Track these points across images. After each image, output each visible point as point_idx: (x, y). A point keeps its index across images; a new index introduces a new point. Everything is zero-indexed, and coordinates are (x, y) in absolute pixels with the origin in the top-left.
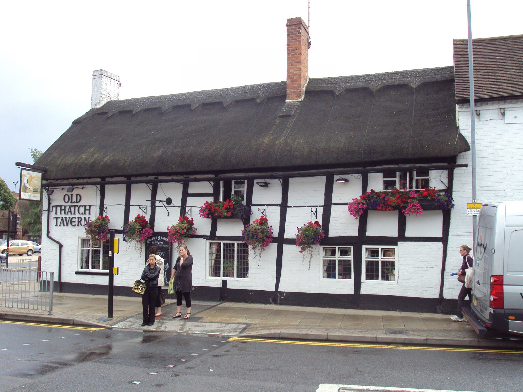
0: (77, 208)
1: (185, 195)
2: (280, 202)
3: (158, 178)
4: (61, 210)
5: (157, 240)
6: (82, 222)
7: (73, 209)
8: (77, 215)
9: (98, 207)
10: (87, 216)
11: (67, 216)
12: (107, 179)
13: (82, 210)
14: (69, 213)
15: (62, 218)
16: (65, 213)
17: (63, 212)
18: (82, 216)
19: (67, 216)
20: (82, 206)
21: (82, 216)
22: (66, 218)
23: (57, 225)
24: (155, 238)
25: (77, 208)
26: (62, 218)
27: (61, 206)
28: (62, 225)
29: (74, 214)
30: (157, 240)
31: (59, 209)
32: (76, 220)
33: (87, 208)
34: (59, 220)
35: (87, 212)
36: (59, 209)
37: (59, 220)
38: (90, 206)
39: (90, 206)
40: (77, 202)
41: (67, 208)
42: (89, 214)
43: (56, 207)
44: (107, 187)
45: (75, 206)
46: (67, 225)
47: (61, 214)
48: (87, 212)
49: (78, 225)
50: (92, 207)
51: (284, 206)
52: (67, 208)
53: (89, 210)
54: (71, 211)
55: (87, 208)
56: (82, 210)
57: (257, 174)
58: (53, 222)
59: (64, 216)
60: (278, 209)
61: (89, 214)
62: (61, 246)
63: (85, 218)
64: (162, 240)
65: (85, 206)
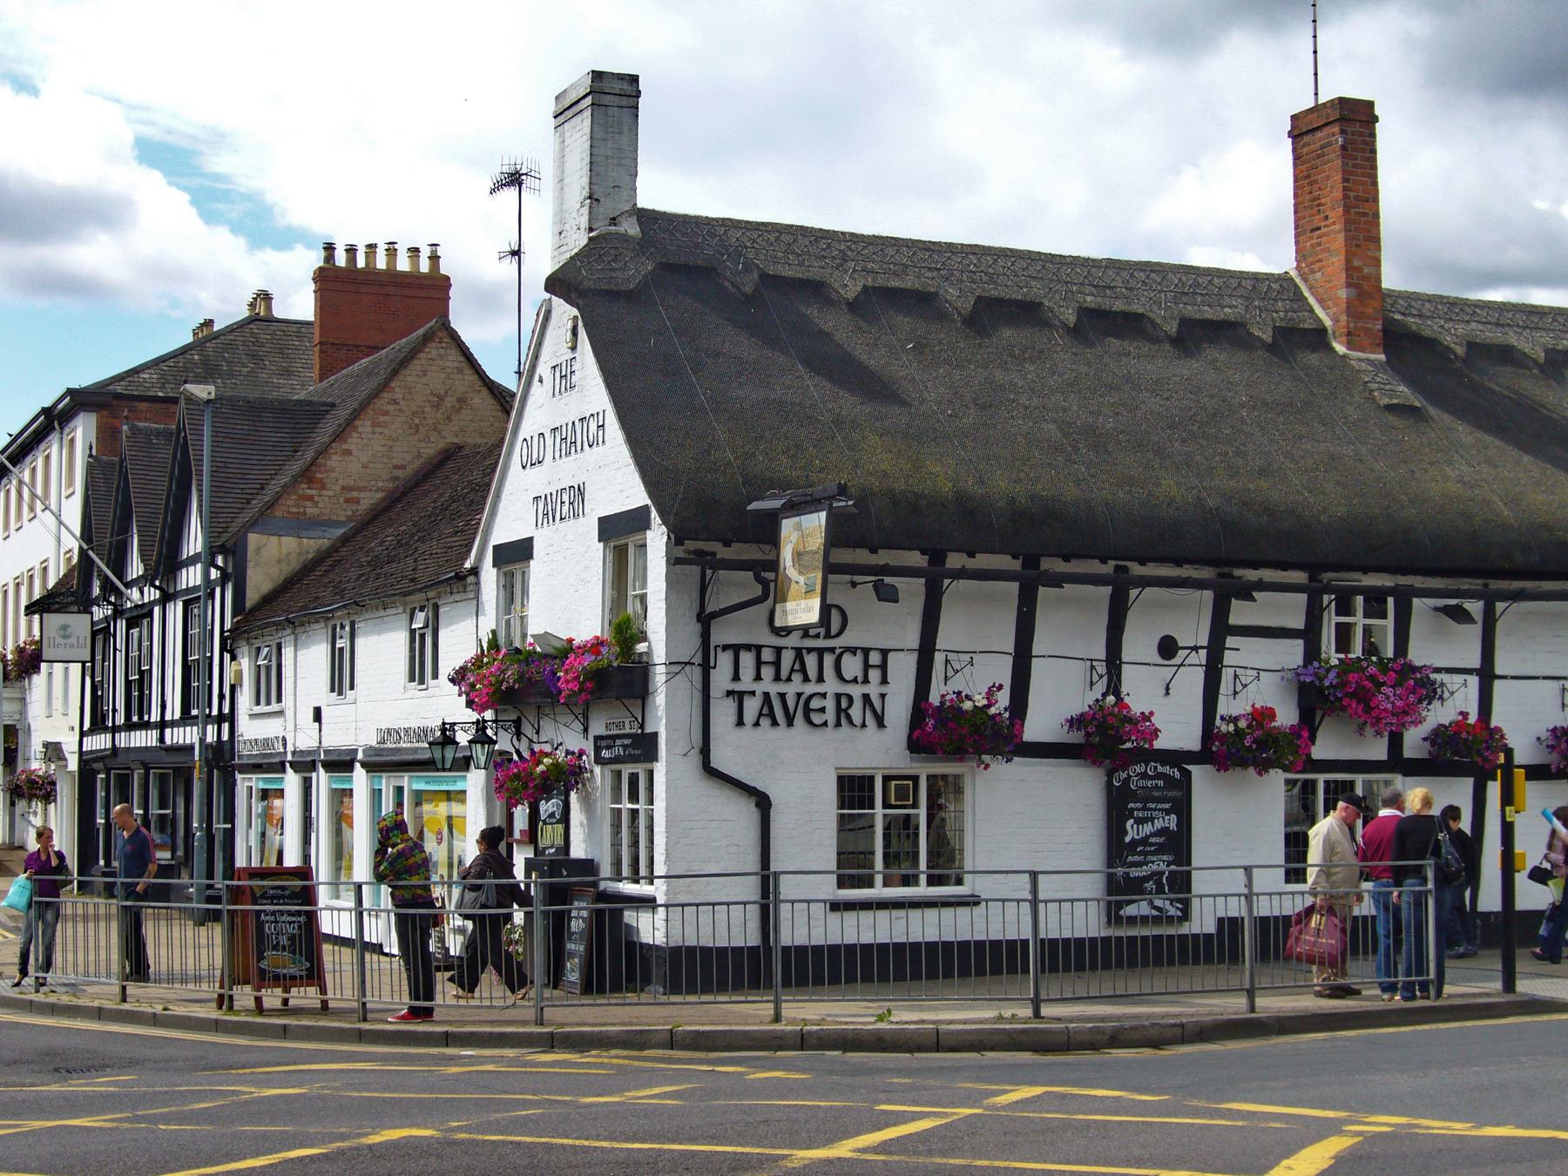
0: (829, 660)
1: (1221, 630)
2: (1475, 662)
3: (1126, 569)
4: (759, 663)
5: (1144, 776)
6: (856, 712)
7: (811, 661)
8: (831, 686)
9: (914, 658)
10: (873, 690)
11: (790, 690)
12: (955, 561)
13: (852, 666)
14: (797, 677)
15: (767, 695)
16: (777, 678)
17: (767, 672)
18: (856, 691)
19: (790, 690)
20: (853, 651)
21: (856, 691)
22: (782, 696)
23: (740, 723)
24: (1139, 769)
25: (829, 660)
26: (767, 695)
27: (758, 649)
28: (765, 722)
29: (820, 679)
30: (1144, 776)
31: (747, 659)
32: (830, 704)
33: (875, 658)
34: (752, 706)
35: (874, 675)
36: (747, 659)
37: (752, 706)
38: (885, 653)
39: (885, 653)
40: (828, 636)
41: (787, 658)
42: (884, 681)
43: (736, 649)
44: (953, 589)
45: (821, 652)
46: (790, 723)
47: (758, 678)
48: (874, 675)
49: (838, 724)
50: (891, 655)
51: (1487, 675)
52: (787, 658)
53: (883, 667)
54: (803, 670)
55: (875, 658)
56: (852, 666)
57: (1418, 582)
58: (723, 712)
59: (774, 689)
60: (1474, 681)
61: (884, 681)
62: (763, 802)
63: (866, 698)
64: (1159, 776)
65: (866, 652)
